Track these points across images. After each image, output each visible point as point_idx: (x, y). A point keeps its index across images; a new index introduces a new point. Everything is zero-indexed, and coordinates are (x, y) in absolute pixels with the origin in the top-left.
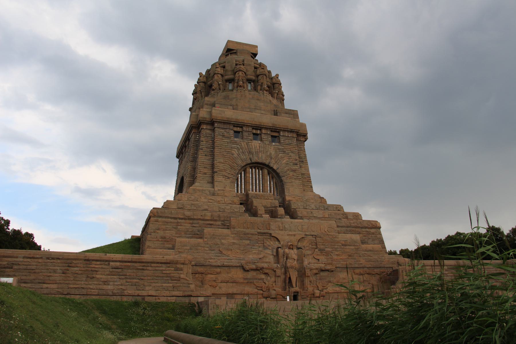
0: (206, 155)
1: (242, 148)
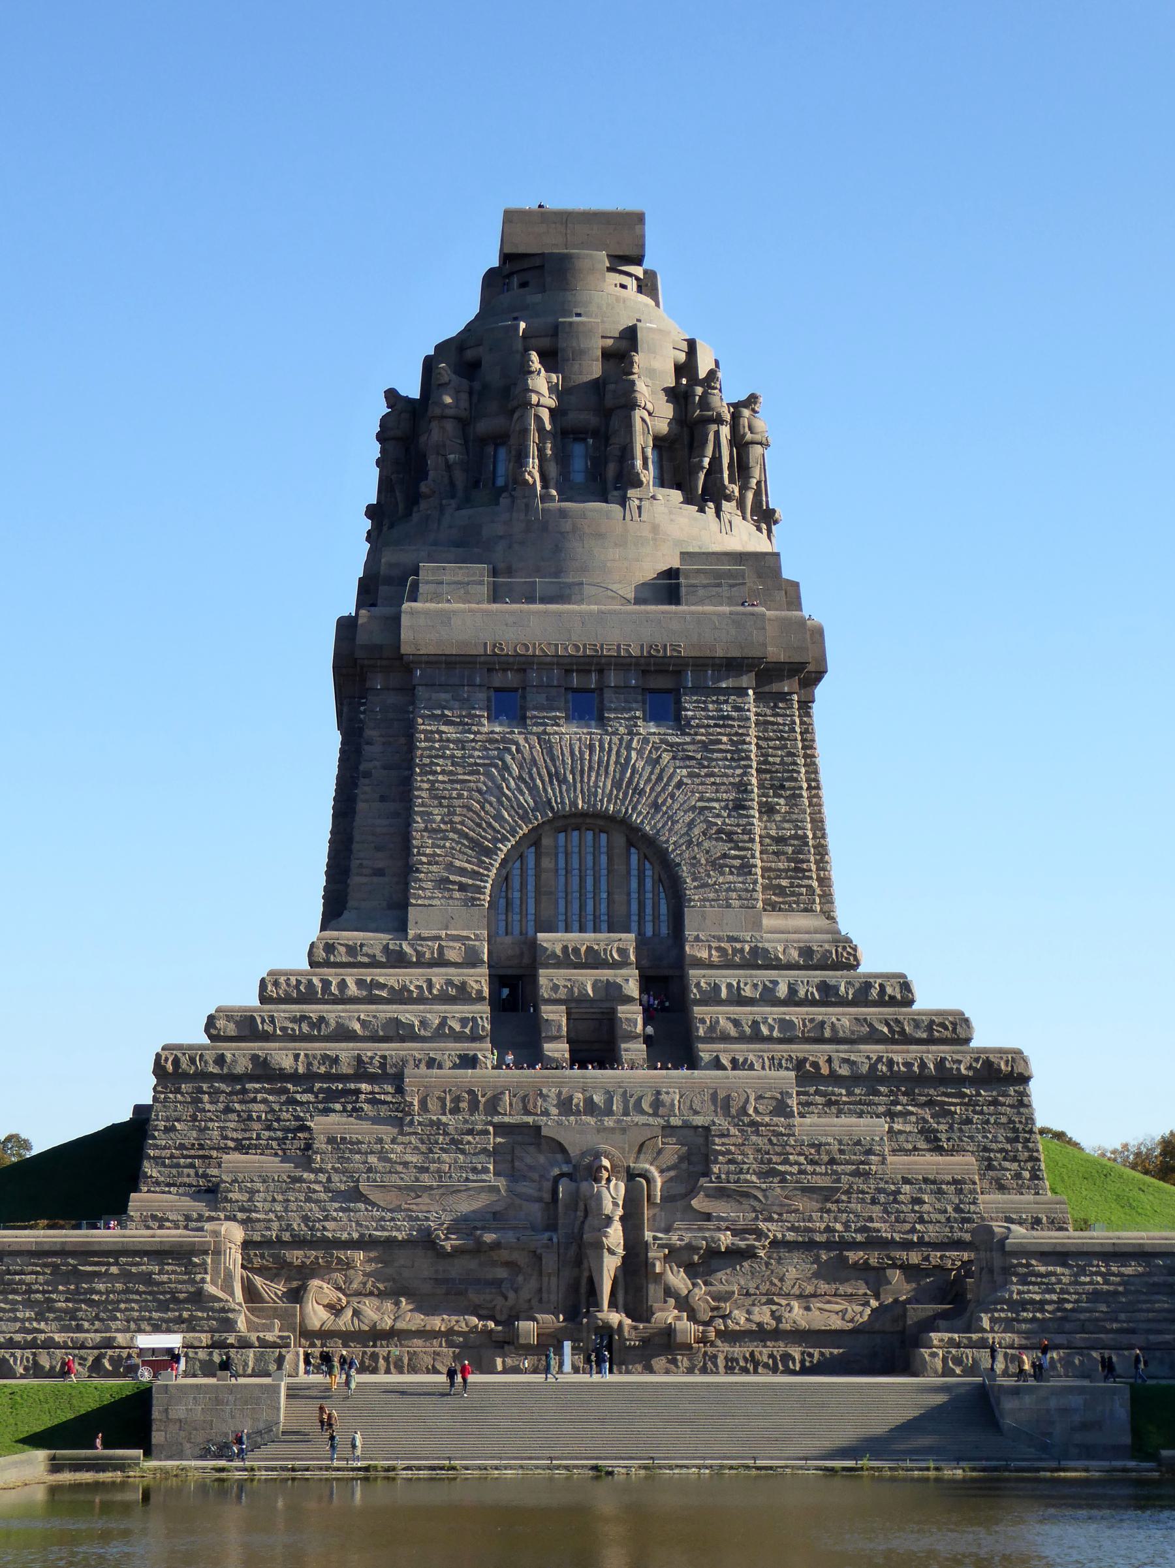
0: (383, 799)
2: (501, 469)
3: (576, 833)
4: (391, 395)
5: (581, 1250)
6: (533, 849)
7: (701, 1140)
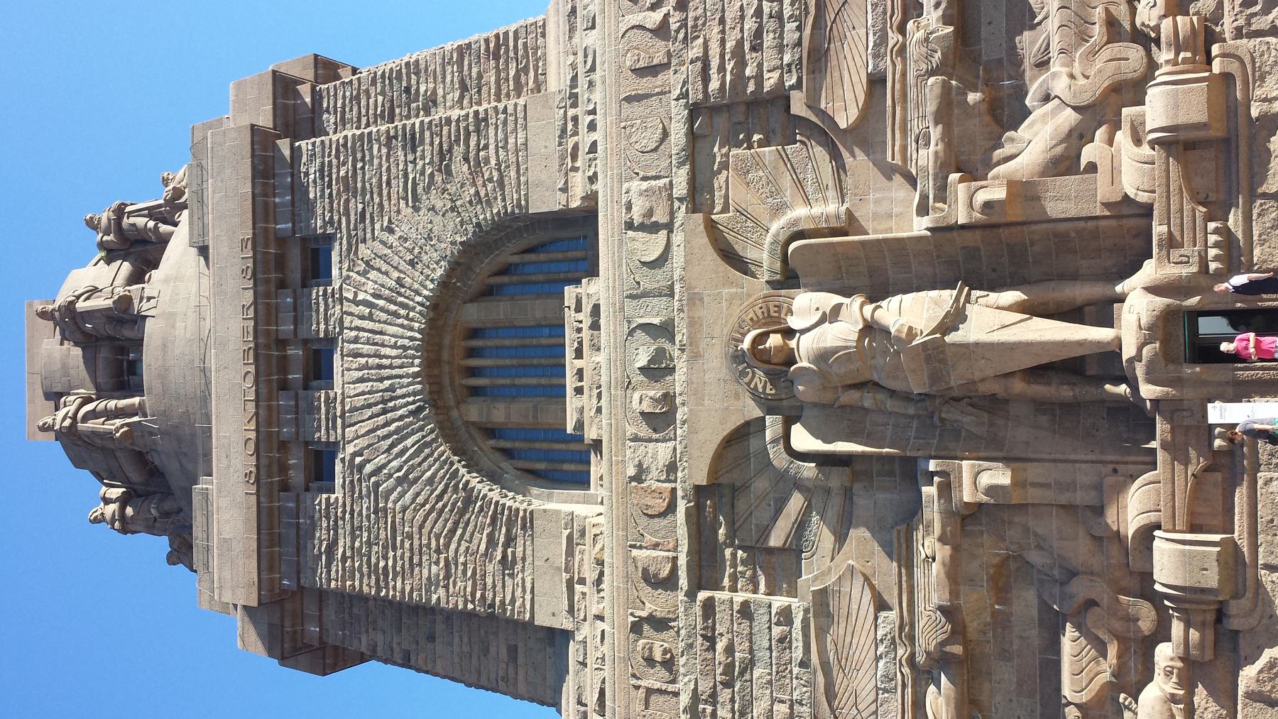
0: (431, 638)
5: (941, 402)
7: (721, 122)
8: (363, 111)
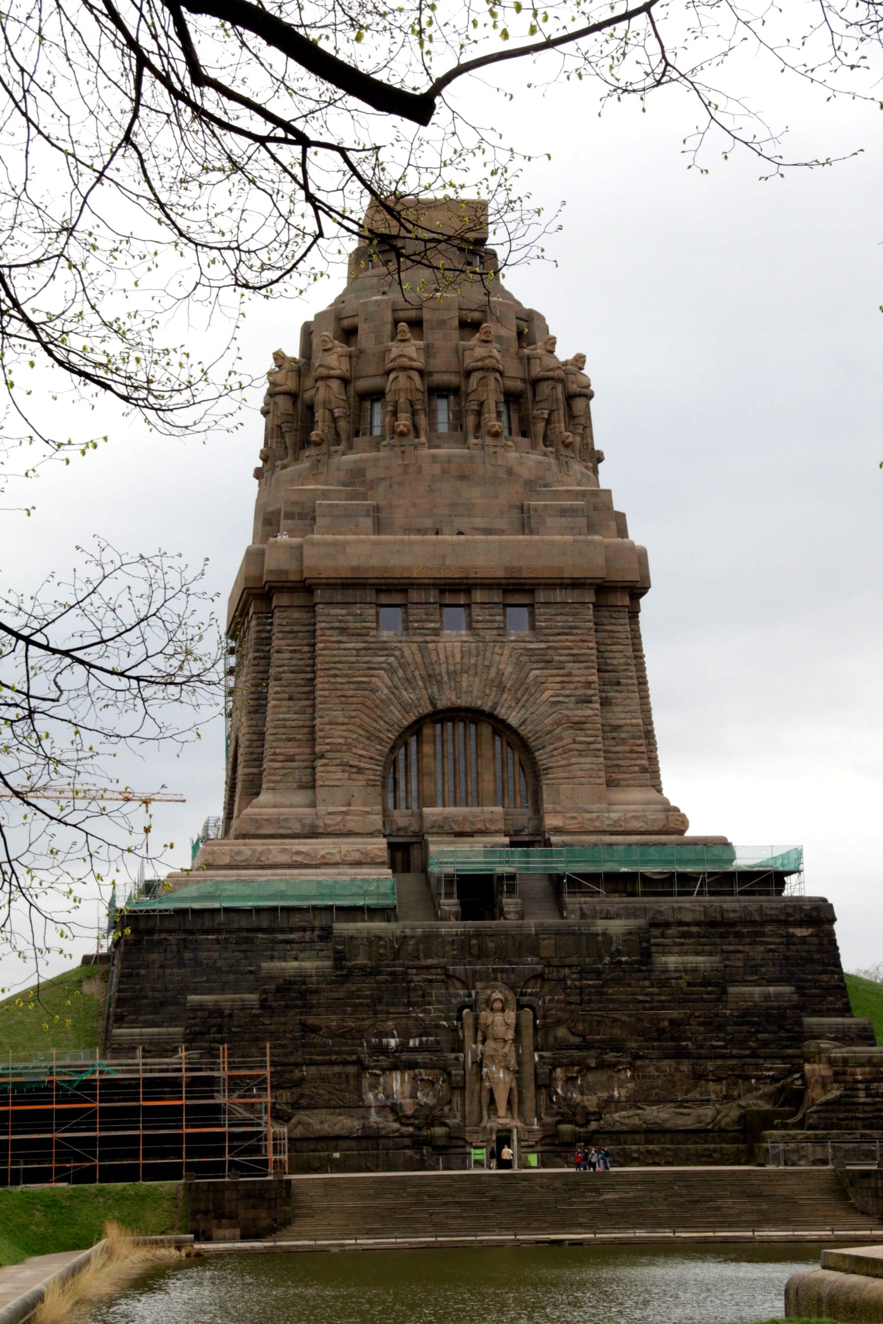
0: (291, 699)
1: (404, 666)
2: (377, 421)
3: (450, 724)
4: (279, 357)
6: (415, 738)
8: (609, 648)
